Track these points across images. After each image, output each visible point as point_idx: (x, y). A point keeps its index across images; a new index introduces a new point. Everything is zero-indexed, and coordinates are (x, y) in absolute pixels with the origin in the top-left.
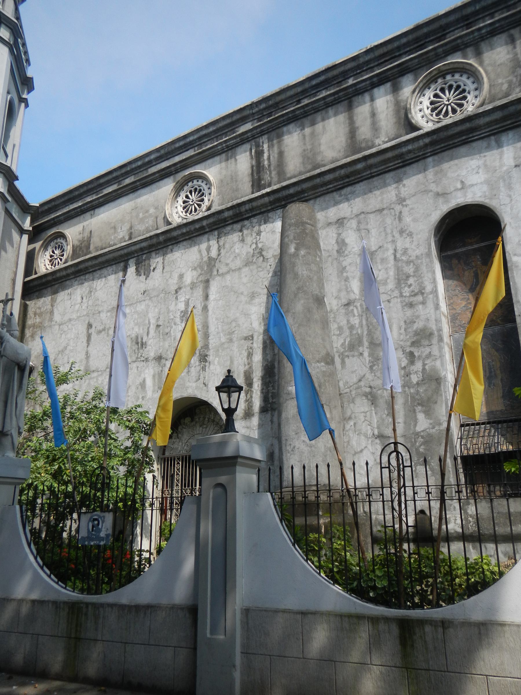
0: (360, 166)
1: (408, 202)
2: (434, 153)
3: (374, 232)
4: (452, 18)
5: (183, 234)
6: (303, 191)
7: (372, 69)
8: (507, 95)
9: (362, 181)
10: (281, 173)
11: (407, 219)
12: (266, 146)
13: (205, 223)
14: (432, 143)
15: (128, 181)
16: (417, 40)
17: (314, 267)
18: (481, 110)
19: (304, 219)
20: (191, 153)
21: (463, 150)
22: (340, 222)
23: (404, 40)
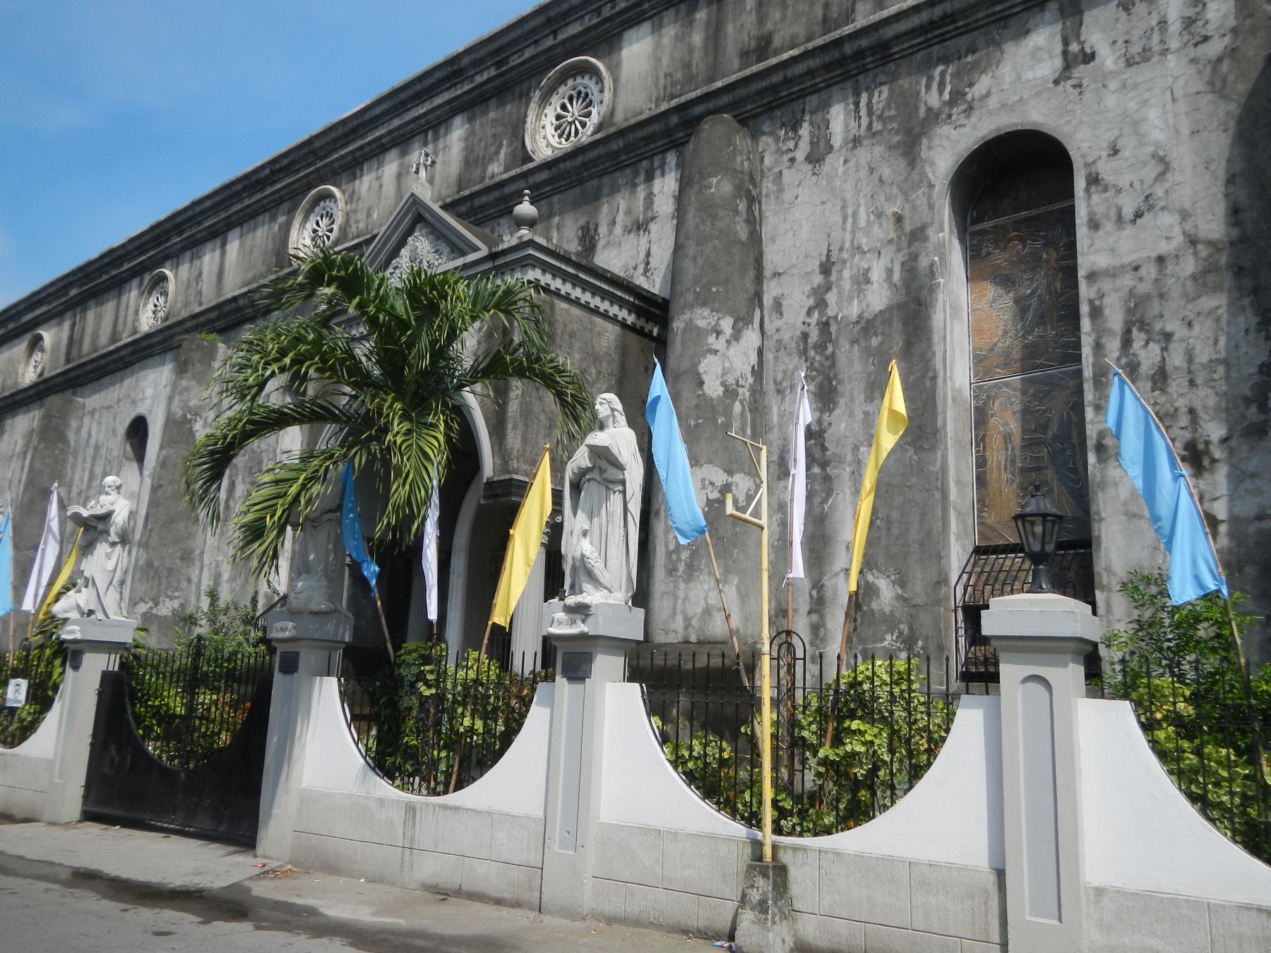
0: (102, 362)
1: (121, 404)
2: (140, 360)
3: (104, 427)
4: (168, 225)
5: (23, 400)
6: (77, 377)
7: (135, 258)
8: (179, 314)
9: (106, 375)
10: (80, 350)
11: (118, 420)
12: (78, 317)
13: (32, 392)
14: (134, 352)
15: (11, 326)
16: (154, 239)
17: (48, 461)
18: (168, 323)
19: (53, 413)
20: (44, 309)
21: (150, 361)
22: (92, 412)
23: (147, 237)
